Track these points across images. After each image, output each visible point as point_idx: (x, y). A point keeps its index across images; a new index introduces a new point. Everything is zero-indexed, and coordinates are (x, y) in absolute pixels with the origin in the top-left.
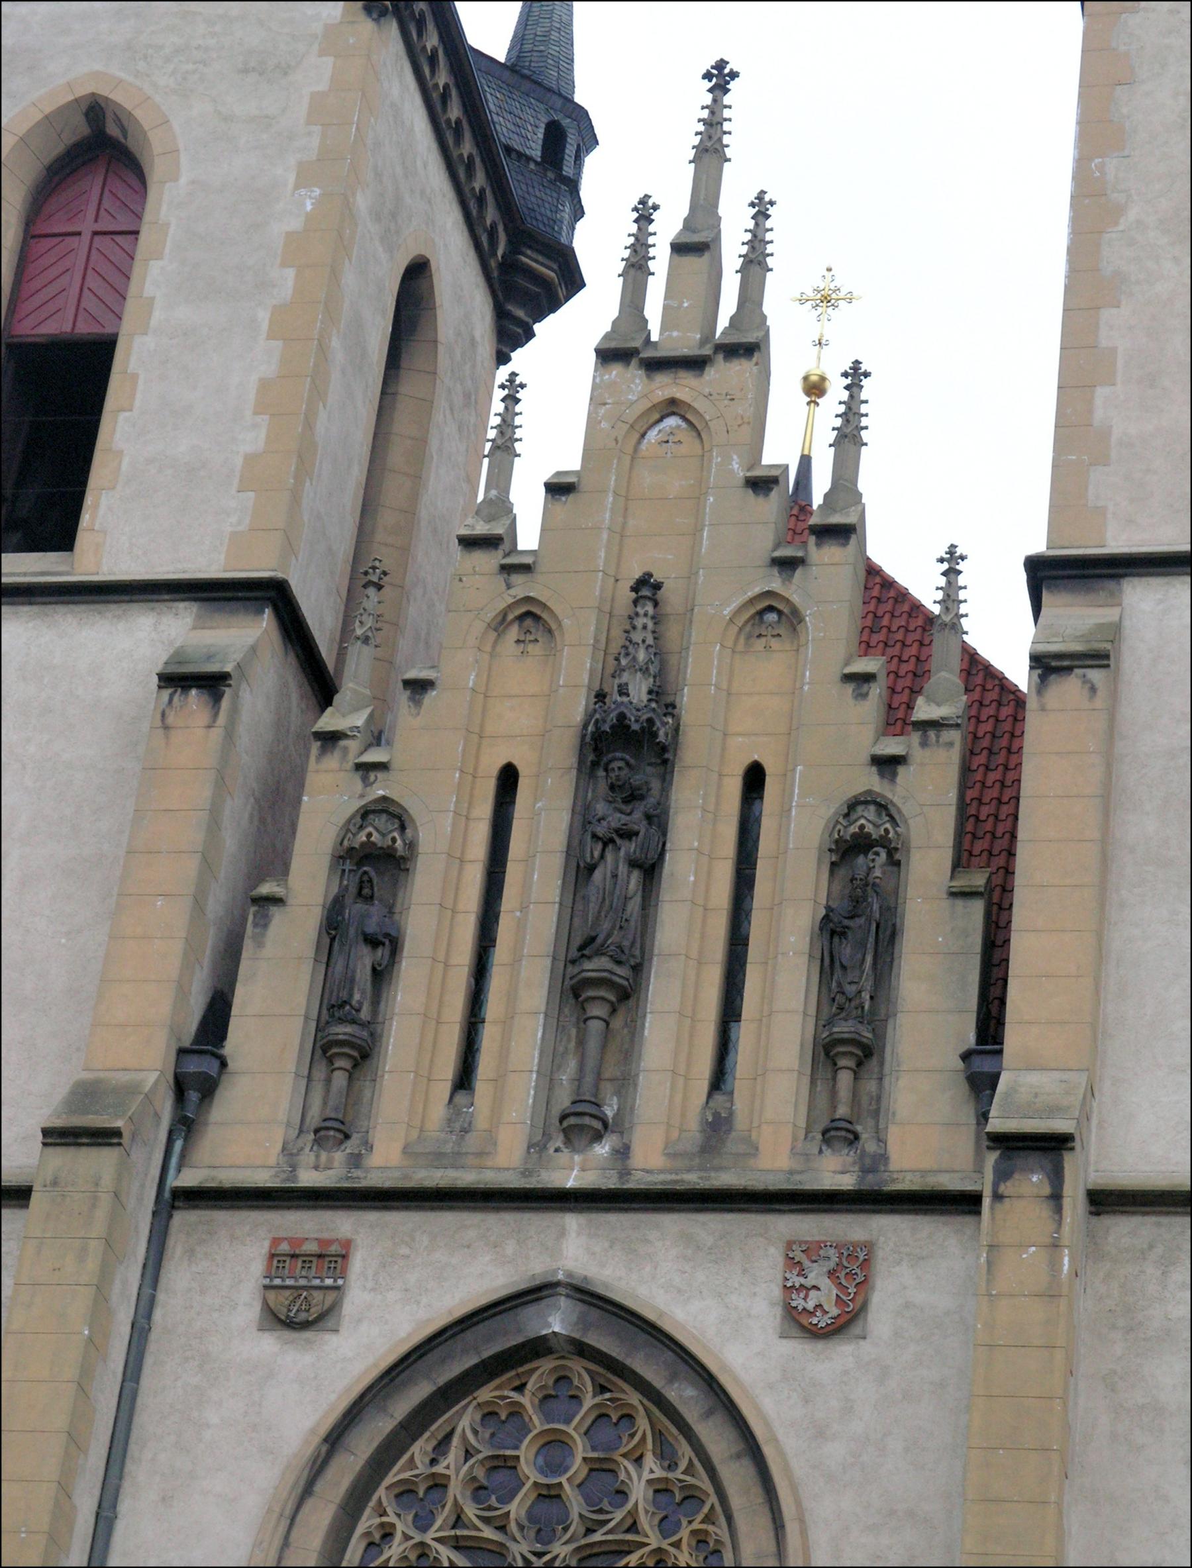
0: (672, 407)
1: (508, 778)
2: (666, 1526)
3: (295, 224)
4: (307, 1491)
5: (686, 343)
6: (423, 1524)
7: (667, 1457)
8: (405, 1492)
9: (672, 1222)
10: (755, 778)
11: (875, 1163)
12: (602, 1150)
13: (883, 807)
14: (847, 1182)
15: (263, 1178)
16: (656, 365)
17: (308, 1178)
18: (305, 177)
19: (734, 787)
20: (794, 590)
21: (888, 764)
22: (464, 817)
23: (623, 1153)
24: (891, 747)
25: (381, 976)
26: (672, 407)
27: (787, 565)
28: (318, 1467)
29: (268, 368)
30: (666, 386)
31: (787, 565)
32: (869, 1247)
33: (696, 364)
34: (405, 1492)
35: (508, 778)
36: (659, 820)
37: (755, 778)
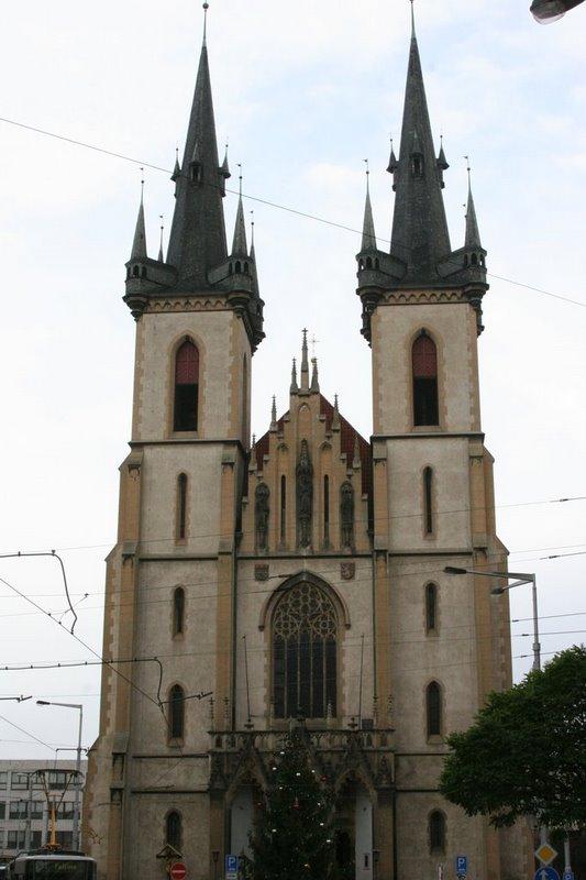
0: (304, 404)
1: (283, 477)
2: (325, 610)
3: (230, 364)
4: (267, 608)
5: (305, 391)
6: (286, 611)
7: (324, 599)
8: (282, 607)
9: (321, 560)
10: (326, 477)
11: (353, 549)
12: (308, 548)
13: (350, 485)
14: (349, 553)
15: (252, 555)
16: (300, 396)
17: (260, 555)
18: (231, 353)
19: (323, 480)
20: (330, 442)
21: (349, 476)
22: (277, 486)
23: (312, 548)
24: (350, 473)
25: (267, 516)
26: (304, 404)
27: (329, 437)
28: (269, 604)
29: (230, 395)
30: (303, 400)
31: (329, 437)
32: (354, 564)
33: (308, 396)
34: (282, 607)
35: (283, 477)
36: (312, 488)
37: (326, 477)
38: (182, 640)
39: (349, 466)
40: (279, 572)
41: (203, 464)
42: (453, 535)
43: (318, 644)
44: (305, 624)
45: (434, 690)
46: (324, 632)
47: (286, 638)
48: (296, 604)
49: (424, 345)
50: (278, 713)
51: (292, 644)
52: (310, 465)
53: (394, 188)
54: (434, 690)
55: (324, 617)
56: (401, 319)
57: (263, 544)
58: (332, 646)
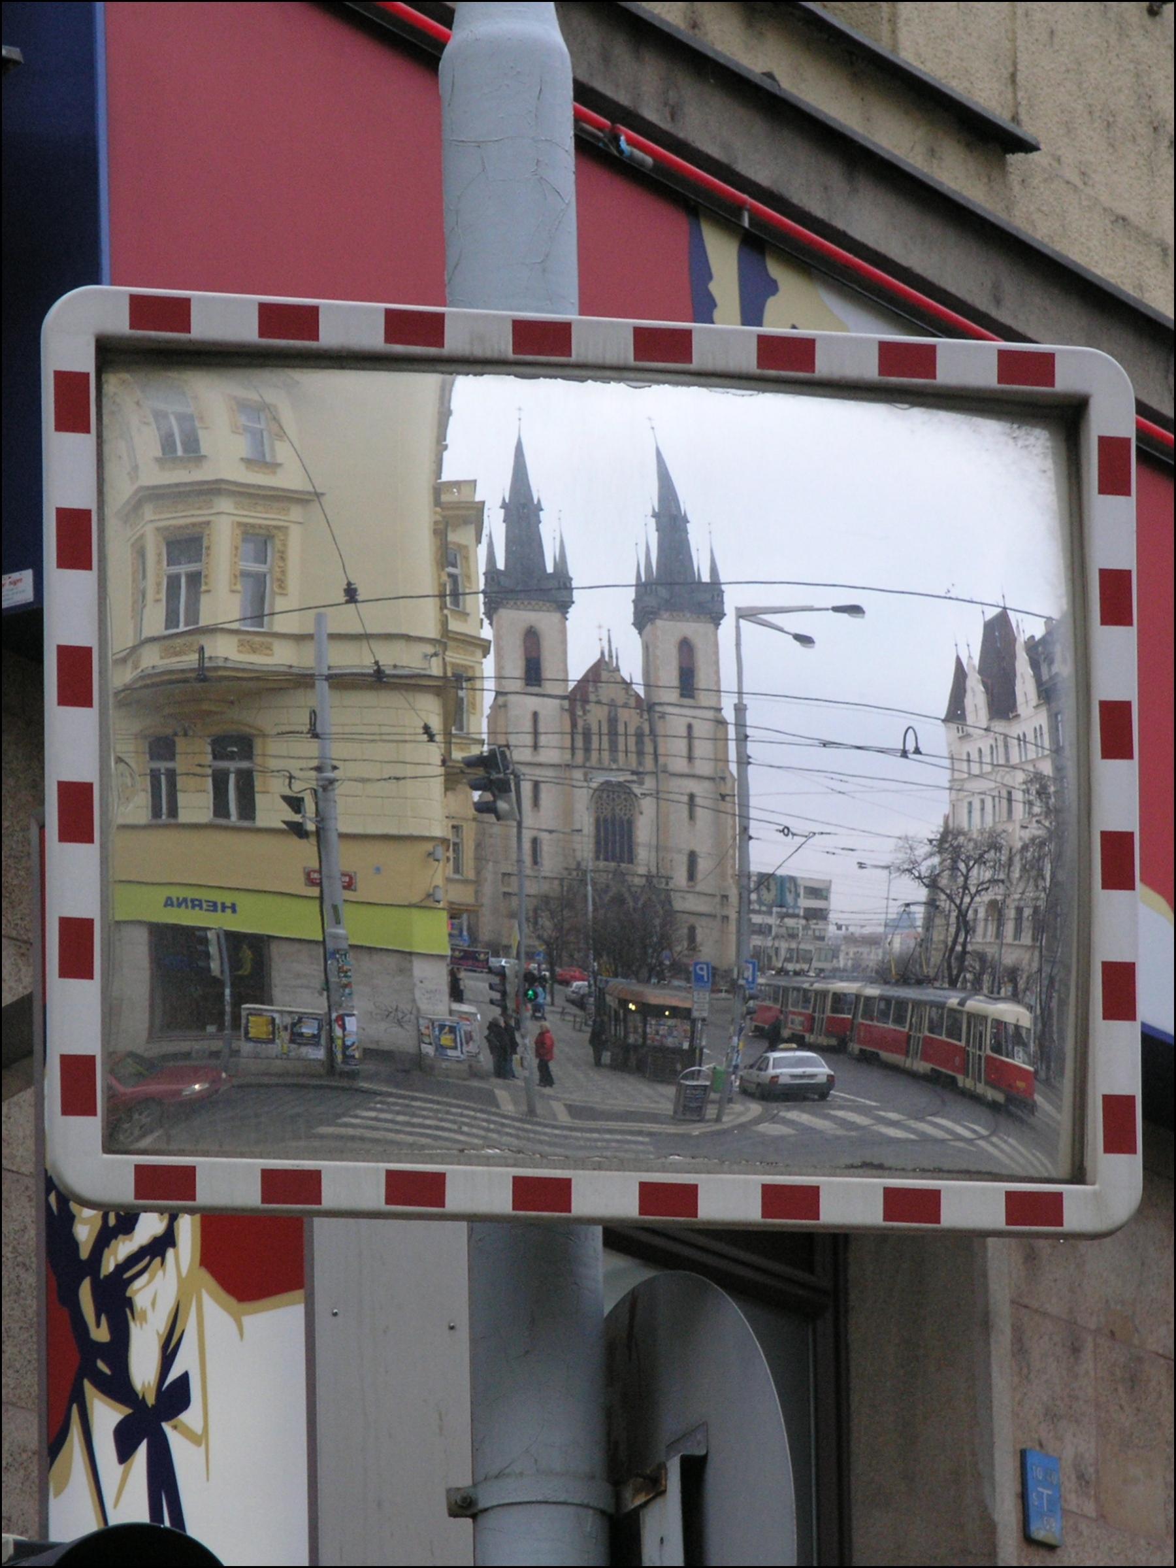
37: (626, 723)
38: (539, 811)
39: (641, 717)
40: (599, 779)
41: (550, 709)
42: (704, 768)
43: (622, 822)
44: (613, 809)
45: (692, 857)
46: (625, 814)
47: (602, 816)
48: (608, 796)
49: (686, 647)
50: (597, 858)
51: (606, 820)
52: (616, 715)
53: (657, 530)
54: (692, 857)
55: (625, 806)
56: (670, 630)
57: (587, 758)
58: (630, 823)
